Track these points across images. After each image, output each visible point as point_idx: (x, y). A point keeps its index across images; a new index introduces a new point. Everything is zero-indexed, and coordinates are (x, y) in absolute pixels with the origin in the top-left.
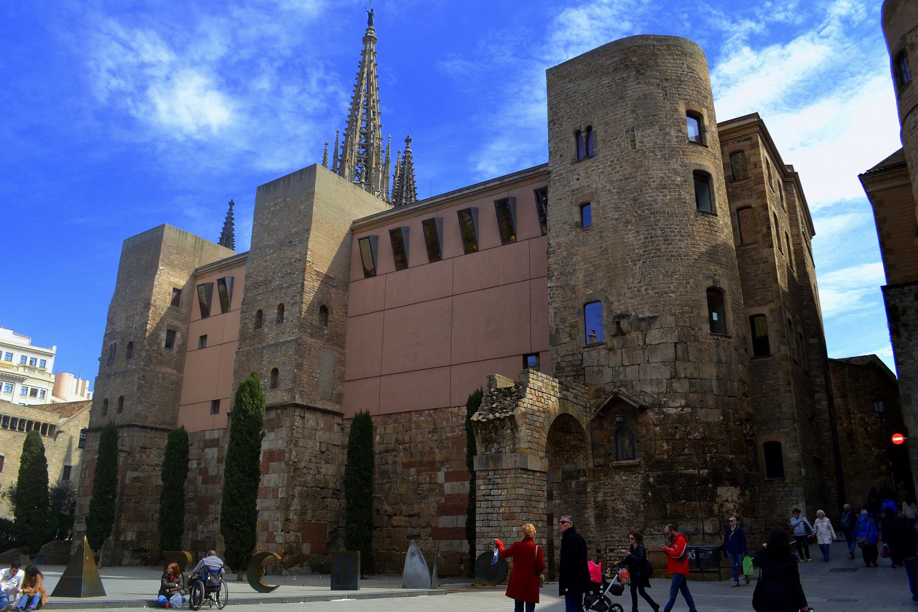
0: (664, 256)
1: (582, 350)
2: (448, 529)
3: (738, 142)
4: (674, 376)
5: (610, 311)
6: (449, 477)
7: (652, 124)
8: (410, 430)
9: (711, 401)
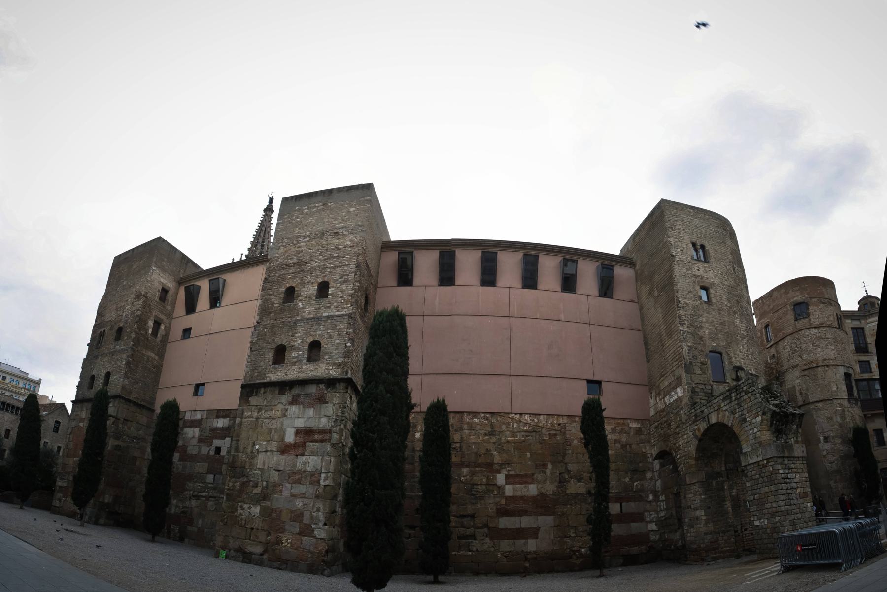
6: (509, 479)
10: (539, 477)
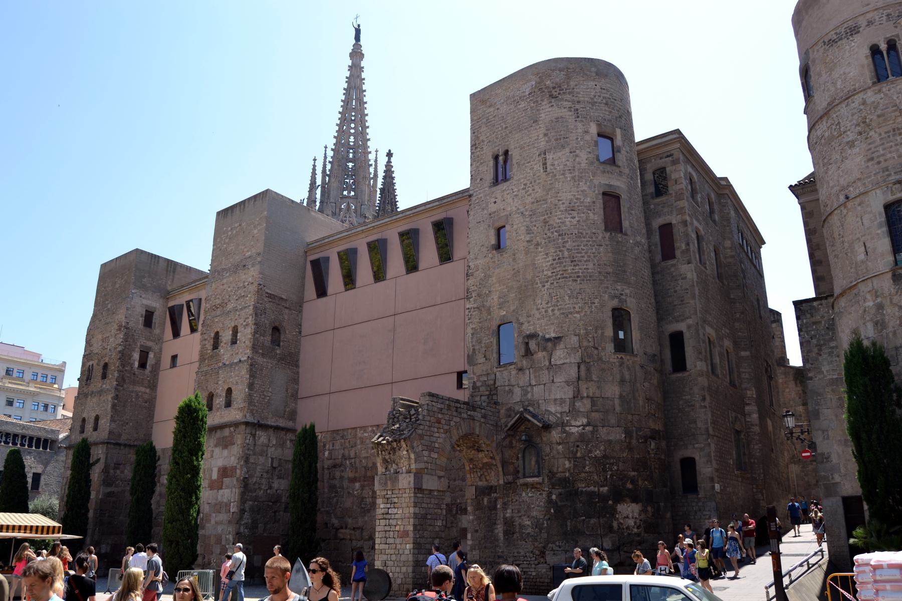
0: (570, 277)
1: (495, 370)
3: (661, 159)
4: (577, 396)
5: (520, 332)
7: (563, 147)
8: (356, 446)
9: (613, 420)
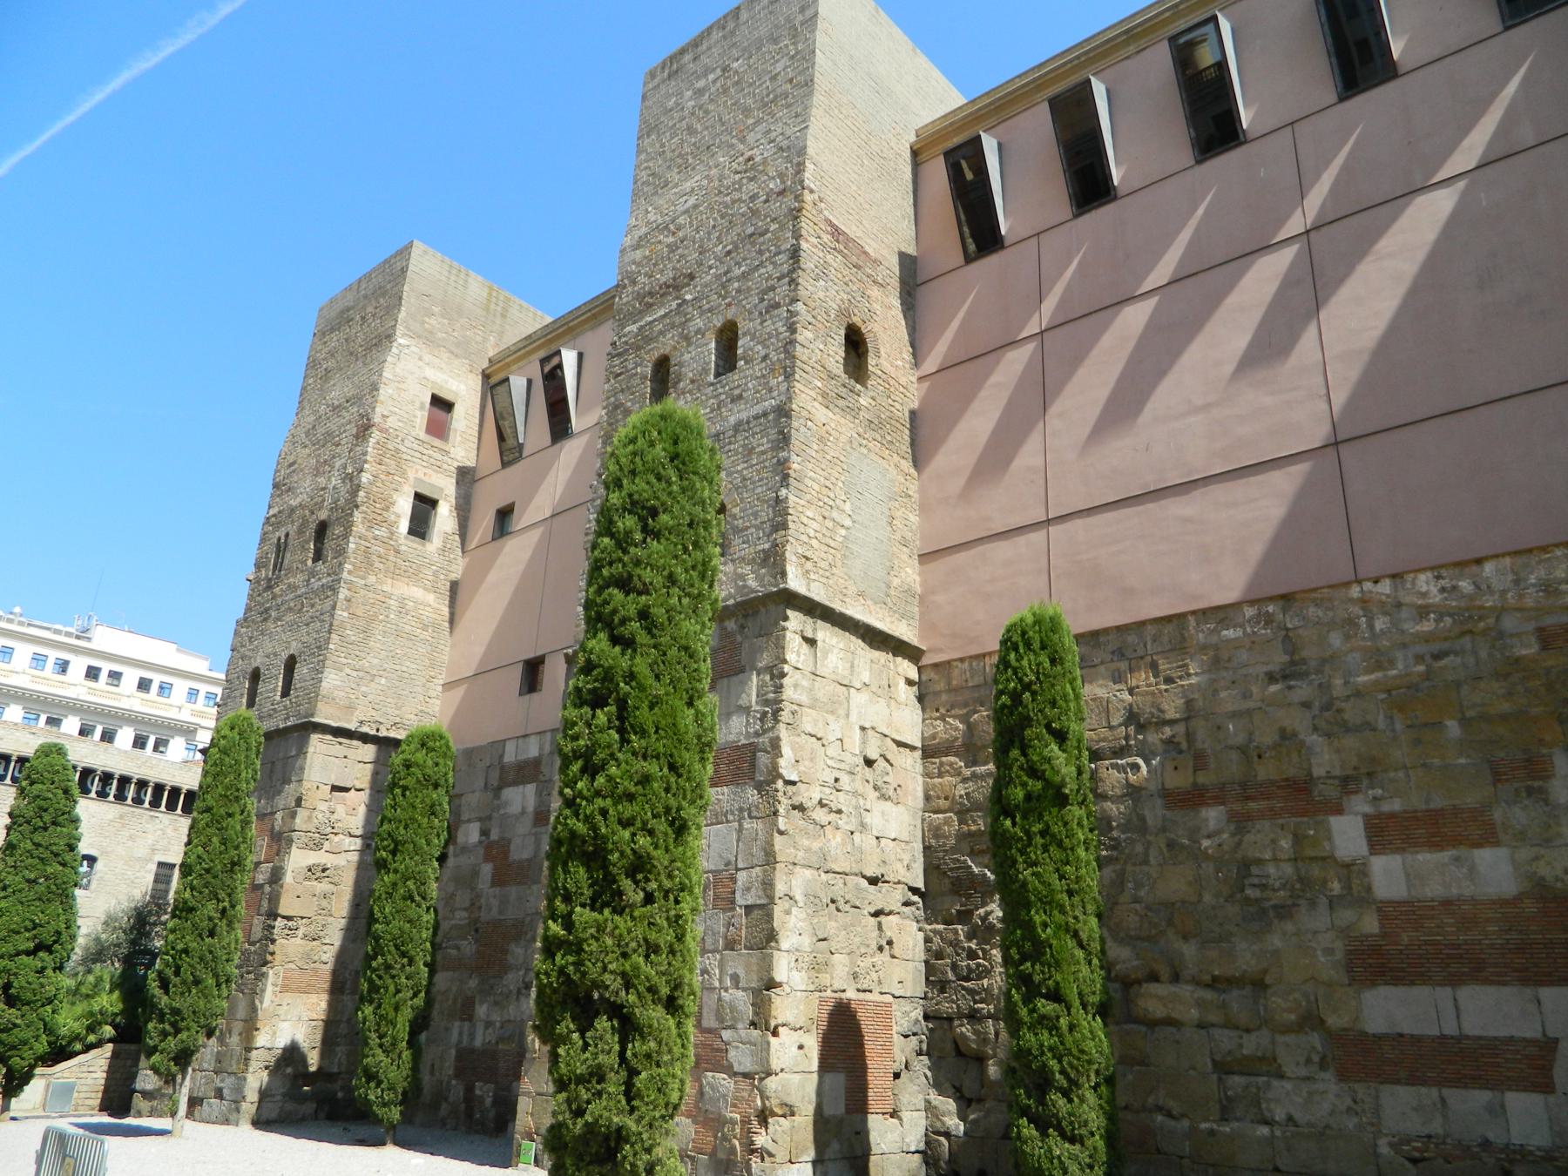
2: (1417, 1040)
6: (1381, 833)
10: (1520, 815)
